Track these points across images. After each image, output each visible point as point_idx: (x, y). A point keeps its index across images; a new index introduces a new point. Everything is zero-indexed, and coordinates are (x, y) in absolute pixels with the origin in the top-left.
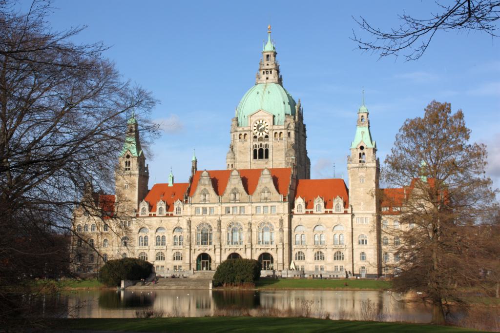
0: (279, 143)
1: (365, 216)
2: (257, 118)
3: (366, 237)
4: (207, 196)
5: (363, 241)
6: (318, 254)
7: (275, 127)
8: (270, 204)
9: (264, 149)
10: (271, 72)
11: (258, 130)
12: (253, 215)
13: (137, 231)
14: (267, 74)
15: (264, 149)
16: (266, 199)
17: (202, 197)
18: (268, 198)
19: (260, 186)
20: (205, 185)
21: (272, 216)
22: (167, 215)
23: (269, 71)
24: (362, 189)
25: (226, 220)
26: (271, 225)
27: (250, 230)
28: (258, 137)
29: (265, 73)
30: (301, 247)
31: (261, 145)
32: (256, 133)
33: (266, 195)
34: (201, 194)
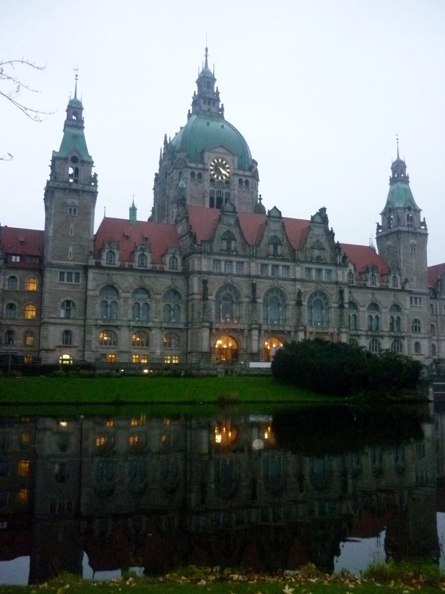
0: (245, 194)
1: (418, 296)
2: (218, 155)
3: (419, 322)
4: (233, 242)
5: (416, 327)
6: (373, 343)
7: (241, 172)
8: (324, 267)
9: (224, 198)
10: (214, 105)
11: (216, 171)
12: (302, 281)
13: (97, 293)
14: (209, 104)
15: (224, 198)
16: (318, 258)
17: (224, 244)
18: (322, 258)
19: (311, 238)
20: (230, 225)
21: (327, 285)
22: (153, 271)
23: (212, 102)
24: (414, 261)
25: (263, 286)
26: (325, 298)
27: (299, 304)
28: (216, 180)
29: (207, 103)
30: (355, 332)
31: (219, 192)
32: (214, 174)
33: (316, 253)
34: (224, 239)
